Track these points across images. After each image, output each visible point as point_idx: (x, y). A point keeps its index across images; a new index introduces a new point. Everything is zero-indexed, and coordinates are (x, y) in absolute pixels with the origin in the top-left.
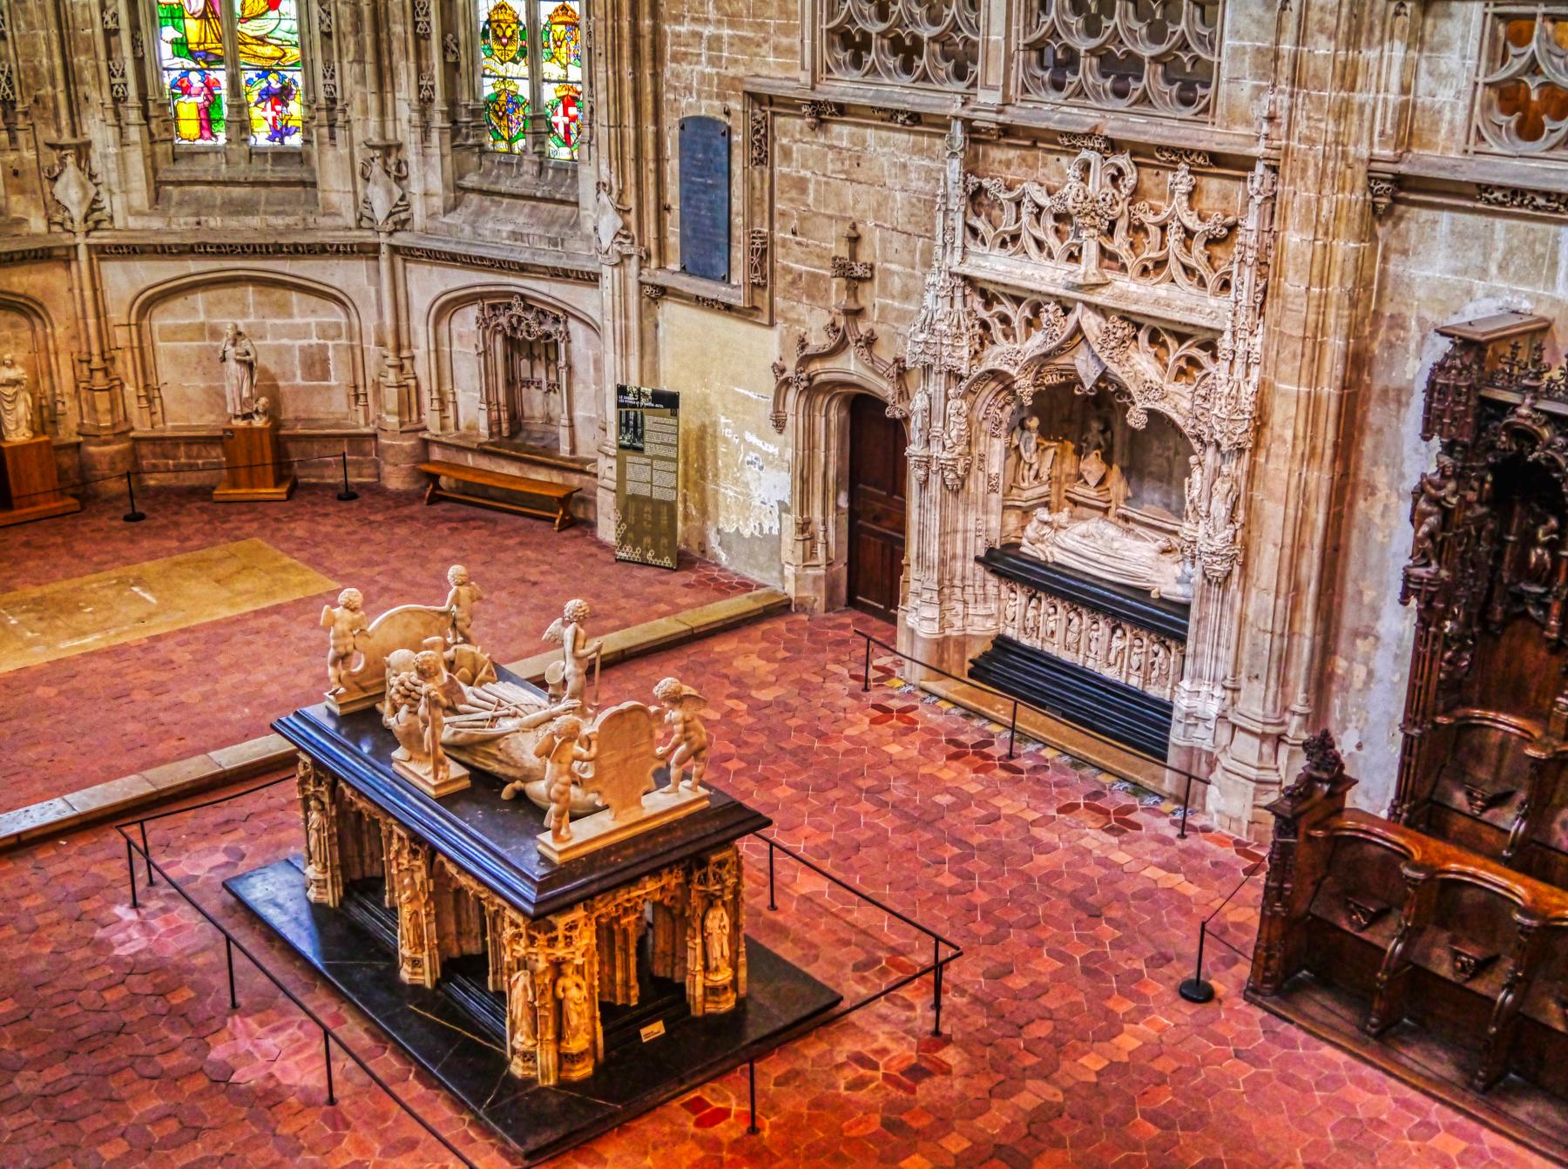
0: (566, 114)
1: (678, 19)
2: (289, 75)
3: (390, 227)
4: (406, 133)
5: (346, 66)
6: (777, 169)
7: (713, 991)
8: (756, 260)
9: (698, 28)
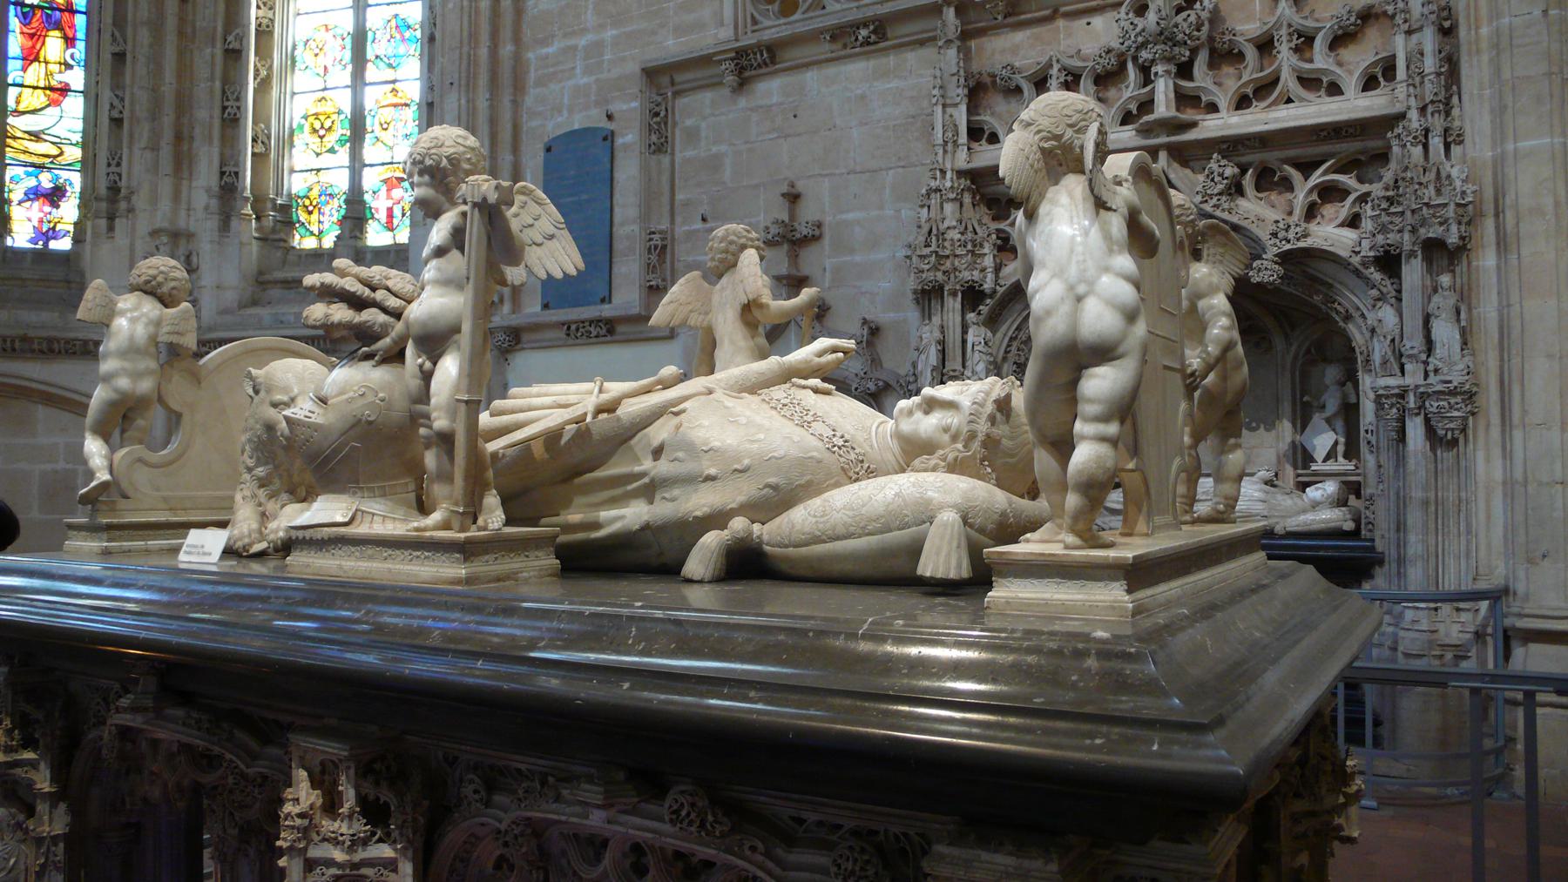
0: (389, 197)
1: (544, 42)
2: (64, 175)
5: (137, 153)
6: (678, 157)
8: (654, 257)
9: (572, 42)
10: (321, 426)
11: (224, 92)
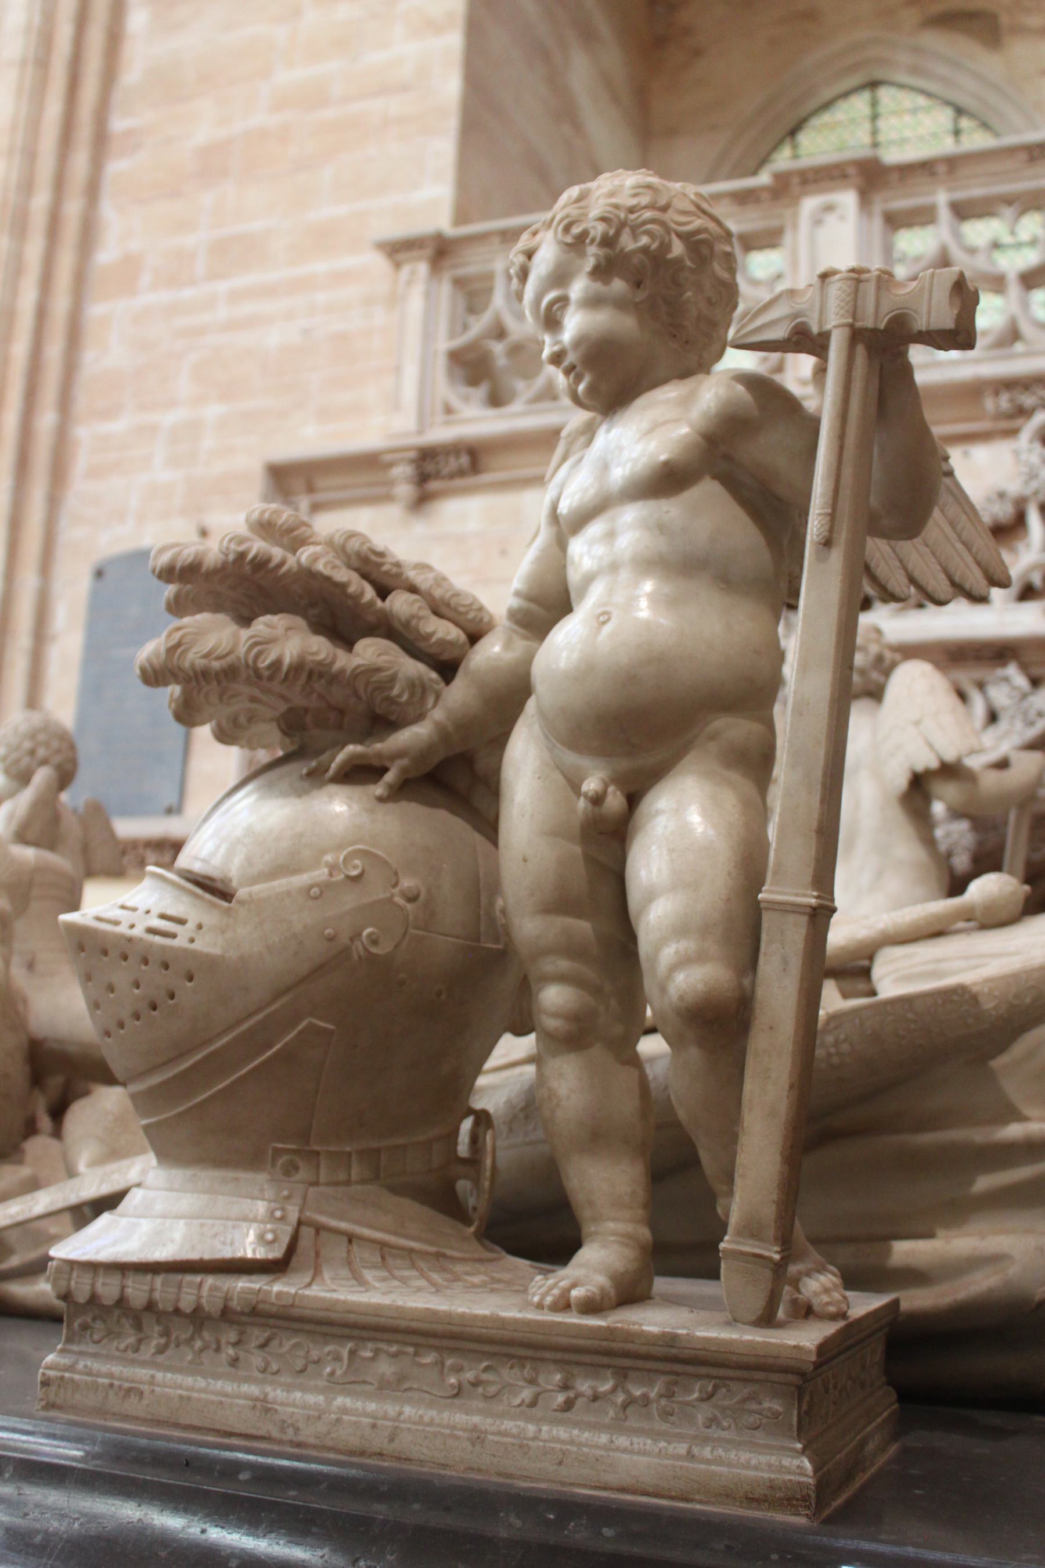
1: (109, 413)
10: (211, 963)
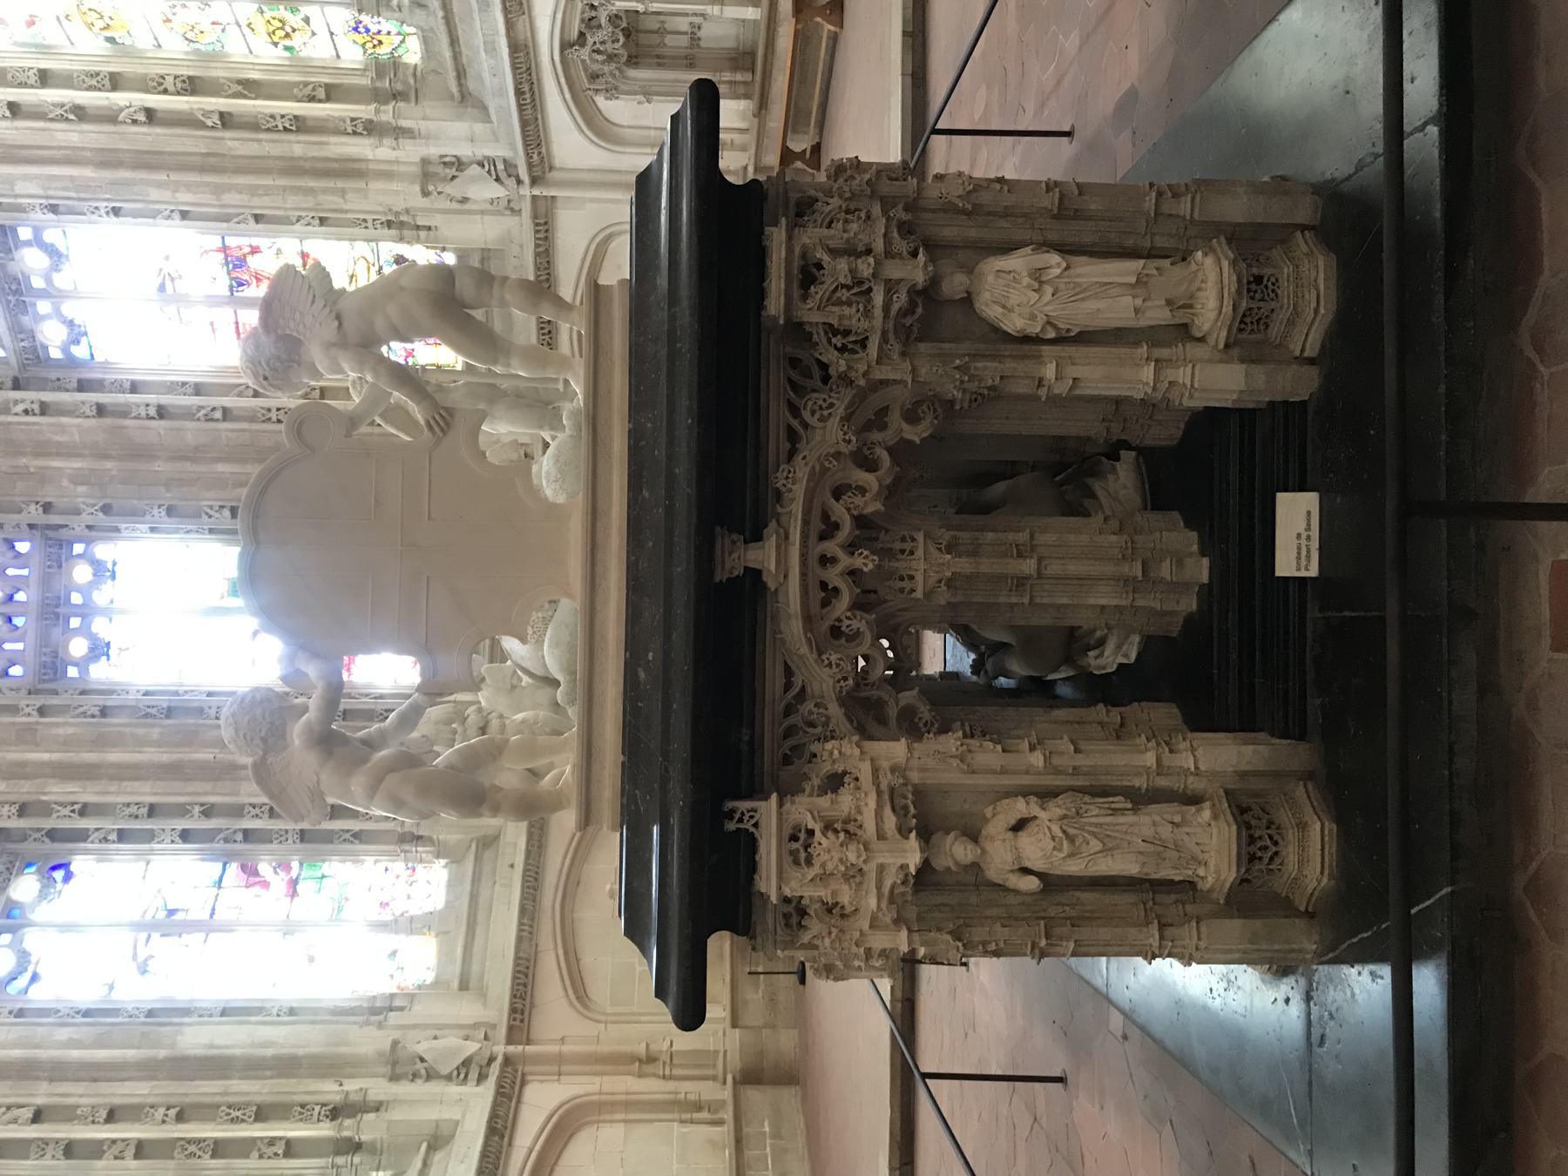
3: (512, 182)
4: (410, 153)
5: (346, 207)
7: (1250, 333)
11: (268, 130)
